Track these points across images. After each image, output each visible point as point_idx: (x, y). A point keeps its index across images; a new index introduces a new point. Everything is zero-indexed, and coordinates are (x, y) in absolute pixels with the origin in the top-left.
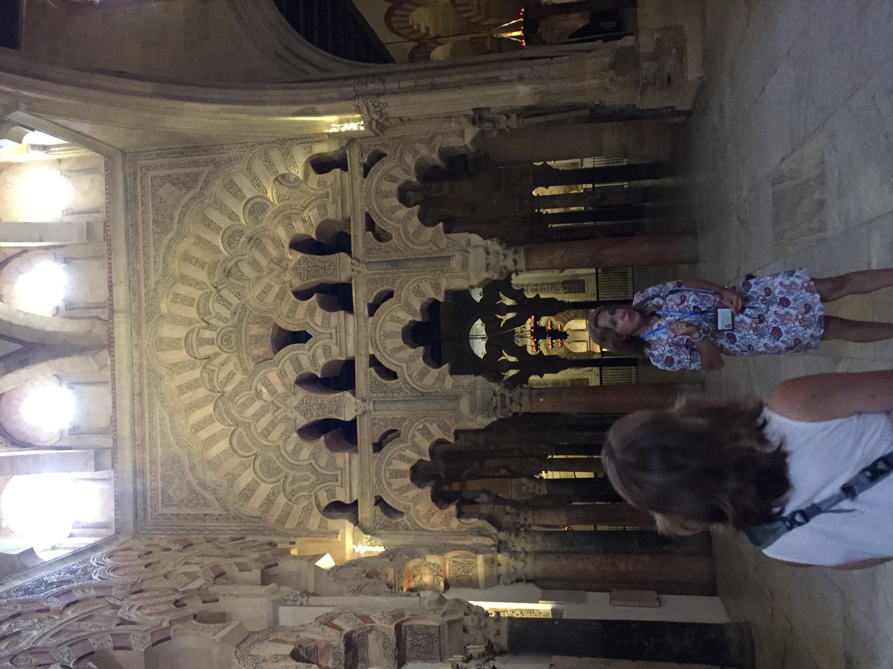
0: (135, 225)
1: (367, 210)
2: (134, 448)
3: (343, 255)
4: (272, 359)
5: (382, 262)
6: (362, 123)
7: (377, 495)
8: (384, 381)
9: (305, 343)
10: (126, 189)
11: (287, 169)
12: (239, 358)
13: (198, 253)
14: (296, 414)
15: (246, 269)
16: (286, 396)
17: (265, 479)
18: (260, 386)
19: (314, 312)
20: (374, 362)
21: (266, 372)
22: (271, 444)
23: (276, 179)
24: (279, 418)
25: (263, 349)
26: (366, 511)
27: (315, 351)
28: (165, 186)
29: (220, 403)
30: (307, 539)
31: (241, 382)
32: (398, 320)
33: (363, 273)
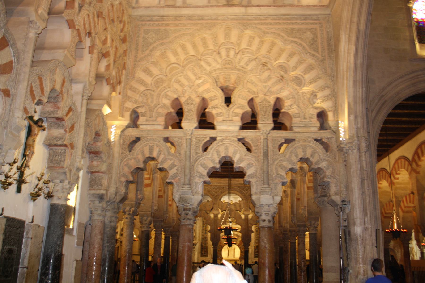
1: (297, 140)
3: (272, 125)
4: (217, 85)
6: (344, 139)
7: (141, 139)
8: (202, 145)
10: (310, 15)
12: (218, 69)
13: (276, 49)
14: (187, 97)
16: (196, 92)
20: (213, 139)
23: (314, 92)
24: (185, 88)
25: (223, 81)
26: (133, 133)
29: (195, 58)
31: (205, 70)
32: (235, 154)
33: (261, 136)
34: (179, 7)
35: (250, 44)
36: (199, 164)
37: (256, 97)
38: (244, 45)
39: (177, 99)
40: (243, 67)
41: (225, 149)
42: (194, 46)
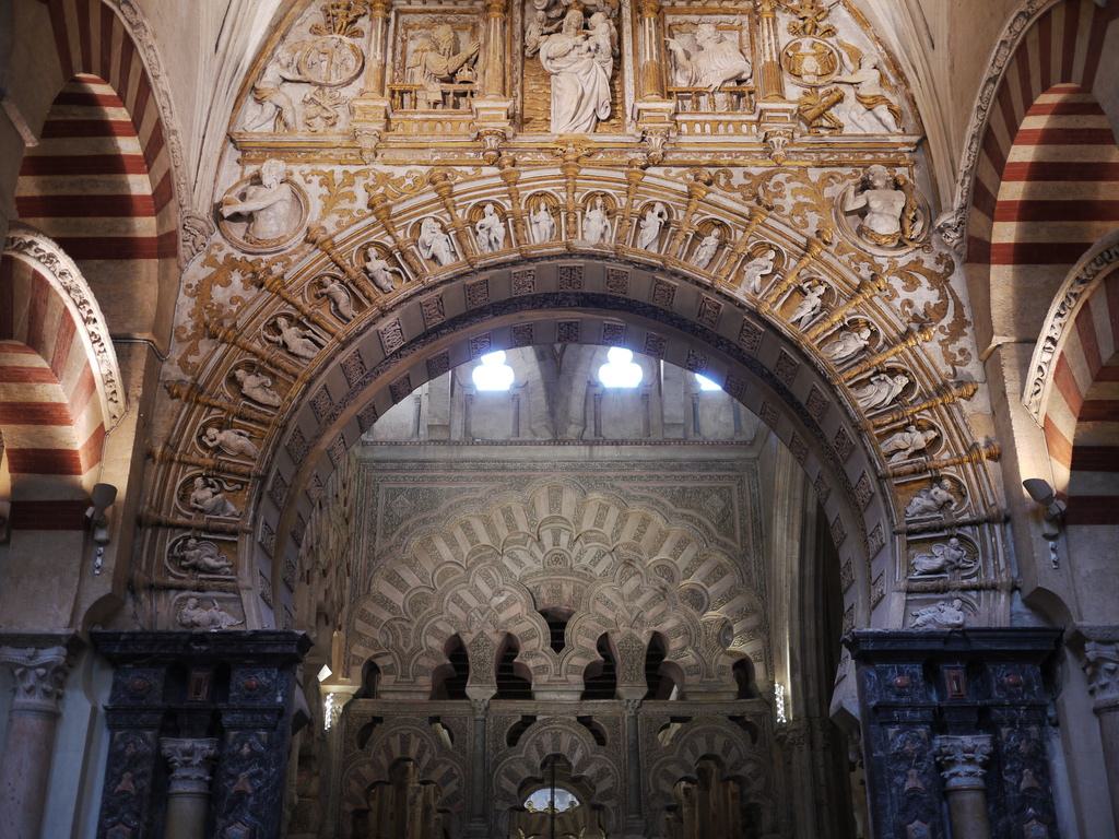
0: (680, 468)
1: (694, 719)
2: (449, 461)
3: (645, 690)
6: (784, 721)
9: (552, 646)
11: (738, 633)
14: (475, 633)
15: (632, 583)
18: (507, 594)
19: (585, 657)
20: (528, 720)
22: (445, 605)
25: (546, 598)
26: (367, 707)
27: (542, 656)
28: (721, 502)
29: (491, 551)
30: (344, 643)
31: (511, 574)
34: (457, 443)
35: (599, 523)
36: (503, 771)
37: (613, 632)
38: (587, 525)
39: (457, 635)
41: (554, 740)
42: (489, 525)
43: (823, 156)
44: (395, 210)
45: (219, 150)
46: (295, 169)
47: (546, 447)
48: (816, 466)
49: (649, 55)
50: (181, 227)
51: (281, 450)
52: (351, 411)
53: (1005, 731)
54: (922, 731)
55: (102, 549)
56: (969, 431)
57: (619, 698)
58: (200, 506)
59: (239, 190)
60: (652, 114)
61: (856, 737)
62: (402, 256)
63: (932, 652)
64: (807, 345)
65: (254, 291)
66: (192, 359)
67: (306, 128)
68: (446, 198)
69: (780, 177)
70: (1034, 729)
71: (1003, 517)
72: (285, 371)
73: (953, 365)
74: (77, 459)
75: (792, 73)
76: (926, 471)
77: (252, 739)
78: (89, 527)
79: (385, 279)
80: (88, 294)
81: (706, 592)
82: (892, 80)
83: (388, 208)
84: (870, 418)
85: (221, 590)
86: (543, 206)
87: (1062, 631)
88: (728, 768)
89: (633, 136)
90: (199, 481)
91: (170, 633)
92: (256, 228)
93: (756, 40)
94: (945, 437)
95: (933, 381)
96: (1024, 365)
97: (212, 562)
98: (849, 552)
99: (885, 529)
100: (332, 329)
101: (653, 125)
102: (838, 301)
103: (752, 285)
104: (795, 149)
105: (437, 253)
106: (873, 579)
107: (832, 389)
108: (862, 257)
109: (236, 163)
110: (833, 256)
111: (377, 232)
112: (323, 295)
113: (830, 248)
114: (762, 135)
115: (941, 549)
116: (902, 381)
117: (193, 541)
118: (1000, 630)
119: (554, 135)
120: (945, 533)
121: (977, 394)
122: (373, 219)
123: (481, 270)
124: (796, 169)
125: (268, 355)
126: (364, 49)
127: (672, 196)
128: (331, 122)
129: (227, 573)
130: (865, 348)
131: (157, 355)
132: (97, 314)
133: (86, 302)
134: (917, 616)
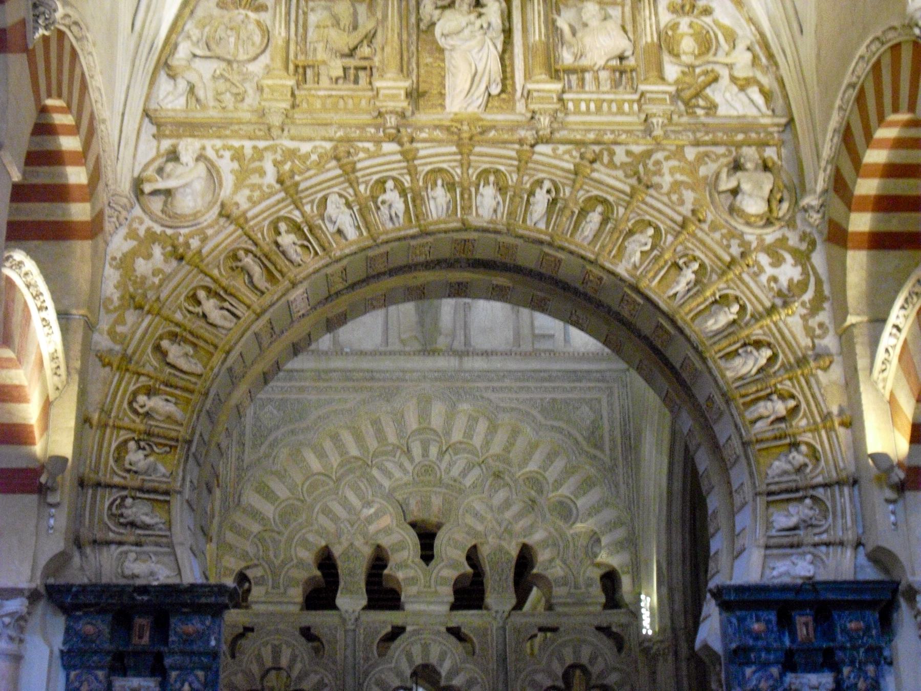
0: (550, 379)
1: (562, 629)
2: (318, 371)
4: (405, 520)
5: (505, 645)
10: (589, 372)
12: (406, 484)
13: (521, 444)
14: (345, 544)
15: (502, 495)
17: (279, 509)
20: (397, 632)
21: (391, 514)
22: (314, 516)
24: (342, 526)
25: (416, 509)
29: (360, 463)
31: (381, 486)
32: (442, 660)
35: (469, 433)
37: (482, 544)
39: (327, 547)
40: (455, 481)
42: (359, 438)
43: (699, 135)
44: (302, 186)
45: (136, 126)
46: (208, 143)
47: (417, 358)
48: (687, 422)
49: (537, 34)
50: (106, 202)
51: (203, 414)
52: (259, 368)
53: (846, 670)
54: (775, 671)
55: (53, 510)
56: (824, 401)
57: (487, 608)
58: (134, 468)
59: (156, 165)
60: (541, 94)
61: (718, 668)
62: (311, 230)
63: (786, 602)
64: (682, 318)
65: (174, 263)
66: (120, 329)
67: (217, 104)
68: (349, 173)
69: (659, 156)
70: (871, 669)
71: (851, 481)
72: (206, 341)
73: (812, 338)
74: (32, 432)
75: (671, 52)
76: (785, 437)
77: (191, 678)
78: (43, 491)
79: (295, 253)
80: (43, 287)
81: (575, 503)
82: (764, 60)
83: (297, 184)
84: (737, 388)
85: (157, 544)
86: (439, 182)
87: (898, 583)
88: (594, 677)
89: (523, 115)
90: (132, 445)
91: (117, 586)
92: (175, 203)
93: (638, 18)
94: (803, 406)
95: (794, 353)
96: (874, 342)
97: (148, 520)
98: (714, 502)
99: (748, 490)
100: (248, 302)
101: (541, 106)
102: (711, 275)
103: (633, 260)
104: (673, 128)
105: (343, 228)
106: (737, 532)
107: (704, 360)
108: (733, 234)
109: (151, 138)
110: (707, 234)
111: (286, 206)
112: (237, 267)
113: (705, 227)
114: (643, 116)
115: (797, 509)
116: (766, 353)
117: (129, 501)
118: (845, 582)
119: (450, 113)
120: (801, 494)
121: (833, 366)
122: (283, 194)
123: (382, 243)
124: (673, 148)
125: (189, 325)
126: (269, 23)
127: (559, 173)
128: (240, 97)
129: (161, 529)
130: (734, 322)
131: (90, 327)
132: (50, 303)
133: (41, 294)
134: (774, 569)
